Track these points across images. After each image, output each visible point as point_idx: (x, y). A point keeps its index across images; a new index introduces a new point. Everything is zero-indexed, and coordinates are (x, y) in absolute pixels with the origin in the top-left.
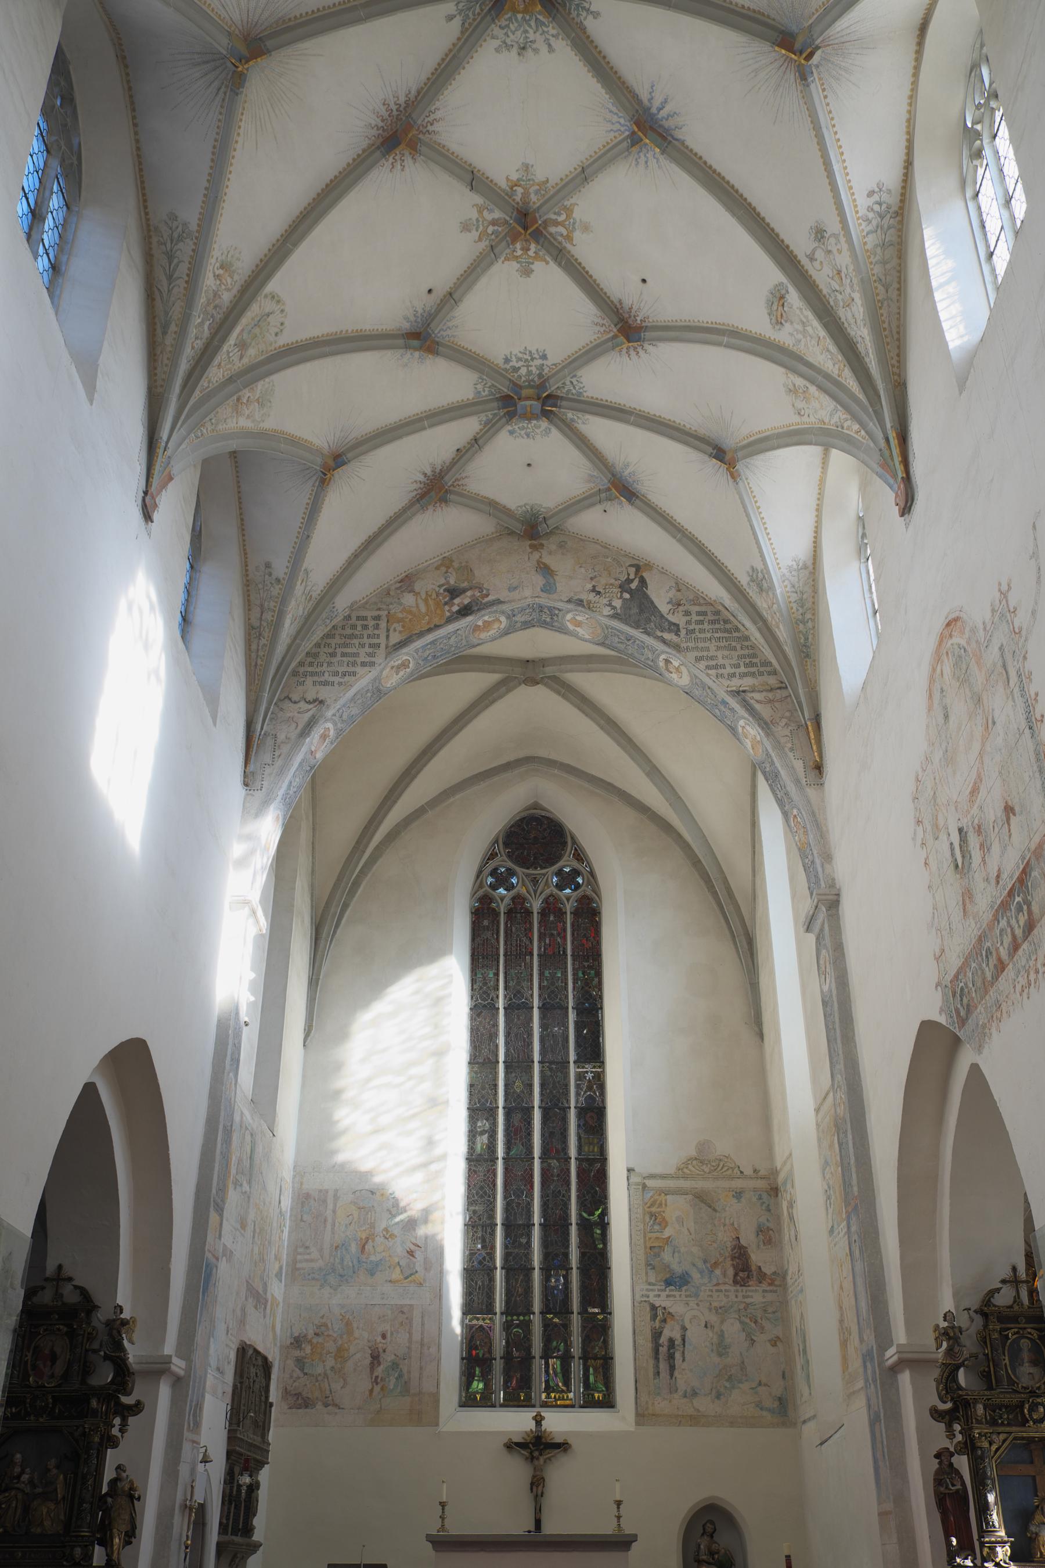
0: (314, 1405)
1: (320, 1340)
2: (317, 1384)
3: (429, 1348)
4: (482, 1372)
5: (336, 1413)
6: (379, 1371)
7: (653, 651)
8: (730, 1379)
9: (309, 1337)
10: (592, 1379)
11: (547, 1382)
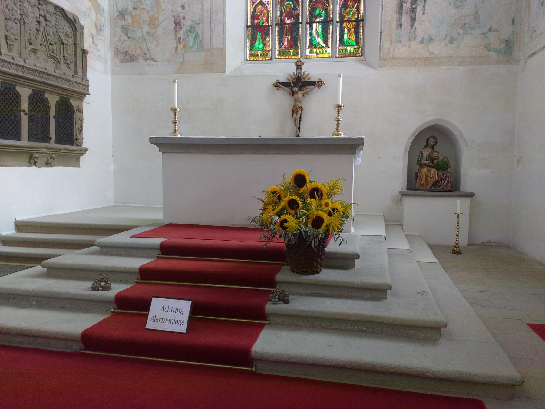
0: (137, 60)
1: (137, 12)
2: (138, 44)
3: (217, 14)
4: (262, 36)
5: (153, 65)
6: (181, 33)
8: (463, 26)
9: (130, 11)
10: (346, 37)
11: (311, 41)
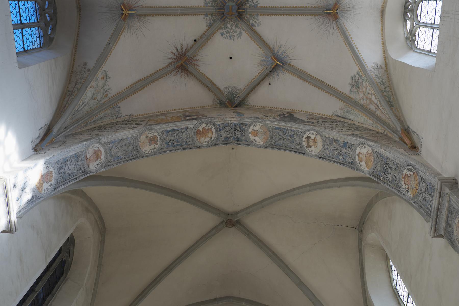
7: (300, 134)
